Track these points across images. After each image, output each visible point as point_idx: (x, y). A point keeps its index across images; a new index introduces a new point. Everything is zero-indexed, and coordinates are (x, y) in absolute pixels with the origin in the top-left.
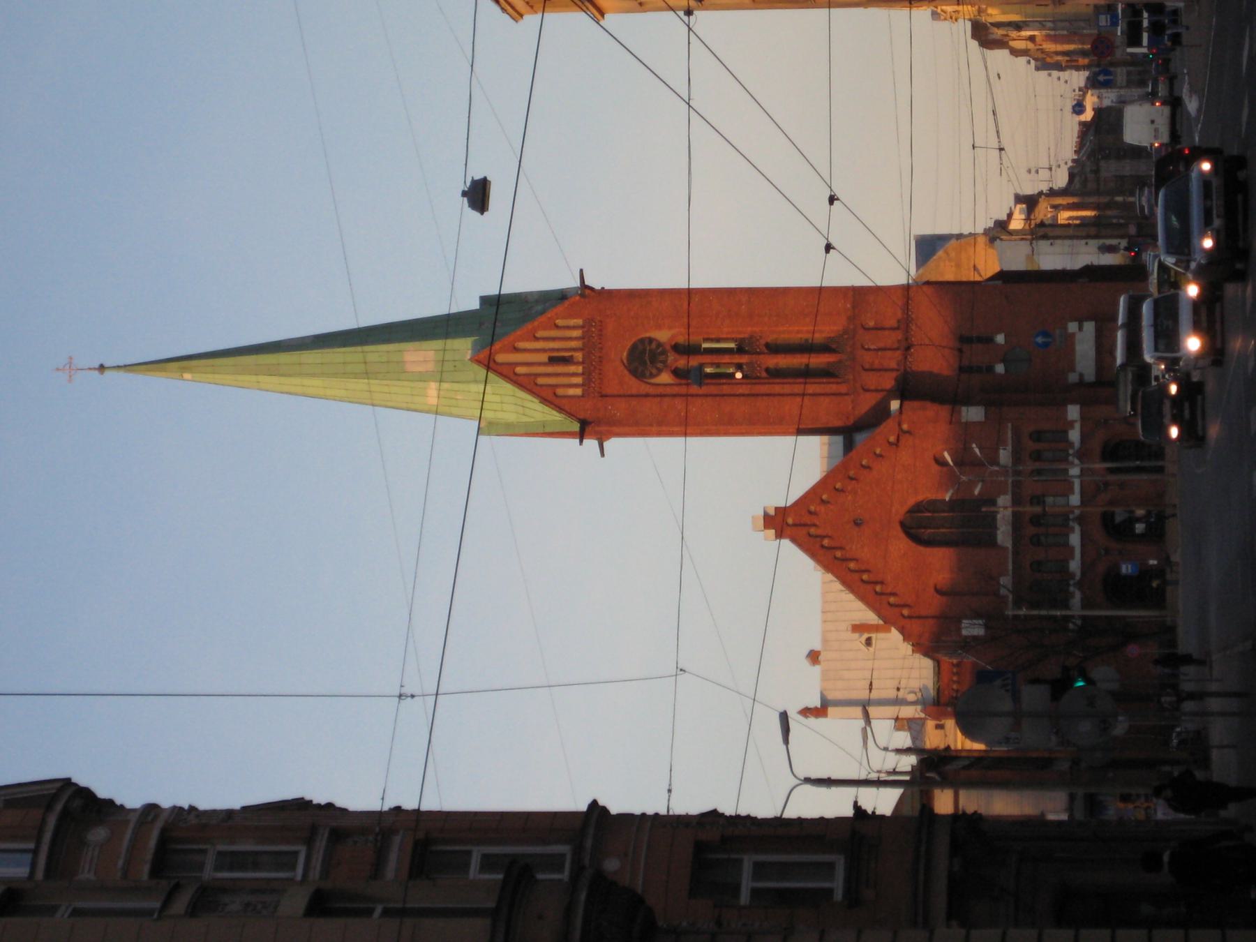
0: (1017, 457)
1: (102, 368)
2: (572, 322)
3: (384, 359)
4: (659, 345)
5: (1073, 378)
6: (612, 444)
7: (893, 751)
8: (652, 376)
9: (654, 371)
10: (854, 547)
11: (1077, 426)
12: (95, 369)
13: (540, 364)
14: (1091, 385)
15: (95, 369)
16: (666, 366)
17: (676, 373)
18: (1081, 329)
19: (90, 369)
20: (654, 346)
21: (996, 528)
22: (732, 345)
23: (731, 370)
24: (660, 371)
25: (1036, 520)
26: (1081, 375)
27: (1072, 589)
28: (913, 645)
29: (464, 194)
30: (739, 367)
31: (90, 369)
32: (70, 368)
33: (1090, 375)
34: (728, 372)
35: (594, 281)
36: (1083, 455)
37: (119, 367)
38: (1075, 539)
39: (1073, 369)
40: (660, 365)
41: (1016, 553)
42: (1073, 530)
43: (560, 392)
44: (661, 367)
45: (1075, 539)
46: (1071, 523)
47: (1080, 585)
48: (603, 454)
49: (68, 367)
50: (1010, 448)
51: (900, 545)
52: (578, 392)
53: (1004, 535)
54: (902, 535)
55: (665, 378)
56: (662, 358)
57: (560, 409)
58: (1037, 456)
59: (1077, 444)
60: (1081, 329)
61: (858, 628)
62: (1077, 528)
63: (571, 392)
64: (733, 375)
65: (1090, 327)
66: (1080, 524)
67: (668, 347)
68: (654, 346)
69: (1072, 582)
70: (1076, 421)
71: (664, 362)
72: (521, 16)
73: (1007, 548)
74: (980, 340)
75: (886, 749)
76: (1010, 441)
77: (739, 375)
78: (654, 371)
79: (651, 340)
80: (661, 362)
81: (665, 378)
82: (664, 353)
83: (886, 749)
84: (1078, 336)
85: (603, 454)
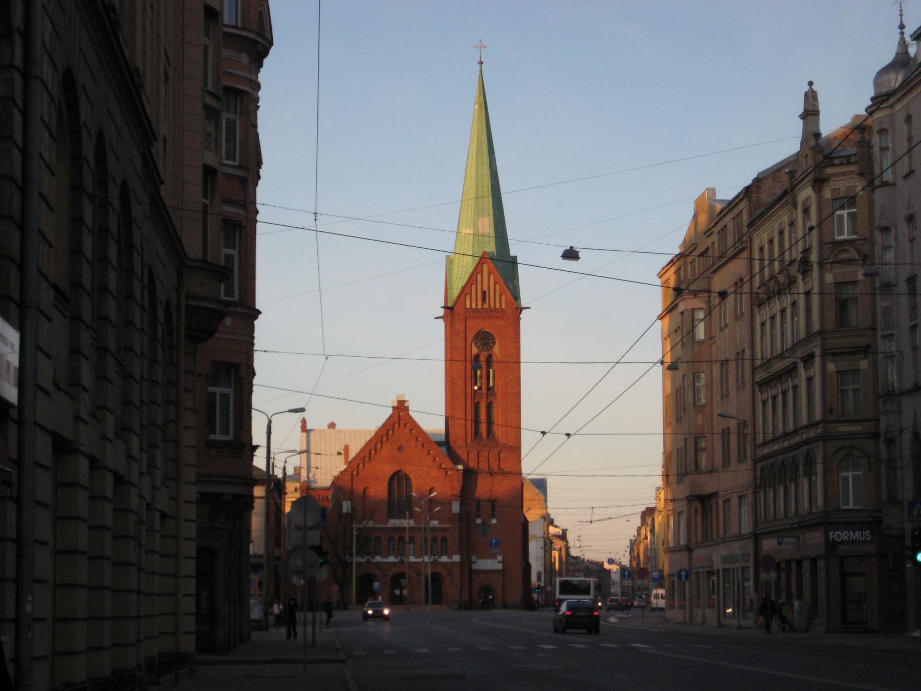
0: (434, 529)
1: (481, 63)
3: (485, 207)
4: (492, 347)
5: (474, 558)
6: (441, 323)
7: (285, 466)
8: (476, 344)
9: (478, 345)
11: (449, 560)
12: (481, 59)
13: (482, 286)
14: (470, 568)
15: (481, 59)
17: (477, 356)
18: (499, 562)
19: (481, 57)
20: (491, 345)
23: (478, 384)
24: (478, 348)
25: (401, 539)
26: (475, 562)
27: (366, 557)
28: (338, 476)
29: (572, 248)
30: (480, 388)
31: (481, 57)
32: (481, 47)
35: (524, 315)
37: (481, 71)
38: (392, 559)
39: (478, 558)
40: (481, 348)
41: (385, 529)
42: (396, 557)
43: (468, 297)
45: (392, 559)
46: (399, 557)
47: (368, 562)
48: (436, 318)
49: (482, 46)
50: (439, 526)
51: (389, 470)
52: (468, 306)
53: (394, 523)
54: (394, 471)
55: (475, 350)
56: (485, 349)
57: (459, 296)
58: (434, 540)
59: (440, 560)
60: (499, 562)
61: (346, 448)
62: (397, 560)
63: (468, 302)
64: (476, 384)
65: (500, 567)
66: (400, 562)
67: (490, 352)
68: (491, 345)
69: (370, 557)
70: (452, 559)
71: (483, 350)
72: (660, 278)
74: (493, 511)
75: (286, 462)
78: (478, 345)
79: (494, 343)
81: (475, 350)
82: (488, 350)
83: (286, 462)
84: (495, 561)
85: (436, 318)
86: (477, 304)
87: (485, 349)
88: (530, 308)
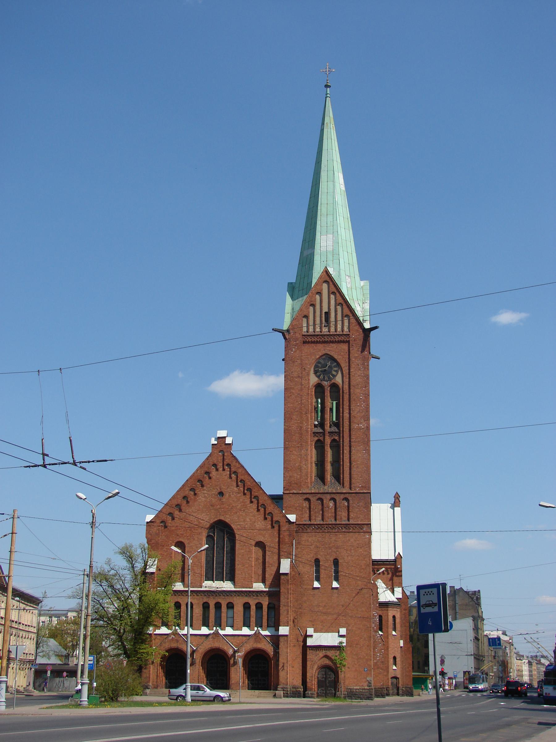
4: (334, 376)
5: (310, 631)
8: (316, 372)
9: (318, 374)
10: (205, 492)
11: (275, 633)
24: (318, 377)
33: (310, 642)
39: (315, 631)
40: (322, 377)
44: (321, 377)
52: (305, 329)
53: (209, 585)
55: (313, 380)
56: (326, 378)
67: (333, 381)
68: (334, 373)
71: (324, 380)
77: (316, 423)
80: (324, 377)
81: (313, 380)
82: (330, 379)
87: (326, 378)
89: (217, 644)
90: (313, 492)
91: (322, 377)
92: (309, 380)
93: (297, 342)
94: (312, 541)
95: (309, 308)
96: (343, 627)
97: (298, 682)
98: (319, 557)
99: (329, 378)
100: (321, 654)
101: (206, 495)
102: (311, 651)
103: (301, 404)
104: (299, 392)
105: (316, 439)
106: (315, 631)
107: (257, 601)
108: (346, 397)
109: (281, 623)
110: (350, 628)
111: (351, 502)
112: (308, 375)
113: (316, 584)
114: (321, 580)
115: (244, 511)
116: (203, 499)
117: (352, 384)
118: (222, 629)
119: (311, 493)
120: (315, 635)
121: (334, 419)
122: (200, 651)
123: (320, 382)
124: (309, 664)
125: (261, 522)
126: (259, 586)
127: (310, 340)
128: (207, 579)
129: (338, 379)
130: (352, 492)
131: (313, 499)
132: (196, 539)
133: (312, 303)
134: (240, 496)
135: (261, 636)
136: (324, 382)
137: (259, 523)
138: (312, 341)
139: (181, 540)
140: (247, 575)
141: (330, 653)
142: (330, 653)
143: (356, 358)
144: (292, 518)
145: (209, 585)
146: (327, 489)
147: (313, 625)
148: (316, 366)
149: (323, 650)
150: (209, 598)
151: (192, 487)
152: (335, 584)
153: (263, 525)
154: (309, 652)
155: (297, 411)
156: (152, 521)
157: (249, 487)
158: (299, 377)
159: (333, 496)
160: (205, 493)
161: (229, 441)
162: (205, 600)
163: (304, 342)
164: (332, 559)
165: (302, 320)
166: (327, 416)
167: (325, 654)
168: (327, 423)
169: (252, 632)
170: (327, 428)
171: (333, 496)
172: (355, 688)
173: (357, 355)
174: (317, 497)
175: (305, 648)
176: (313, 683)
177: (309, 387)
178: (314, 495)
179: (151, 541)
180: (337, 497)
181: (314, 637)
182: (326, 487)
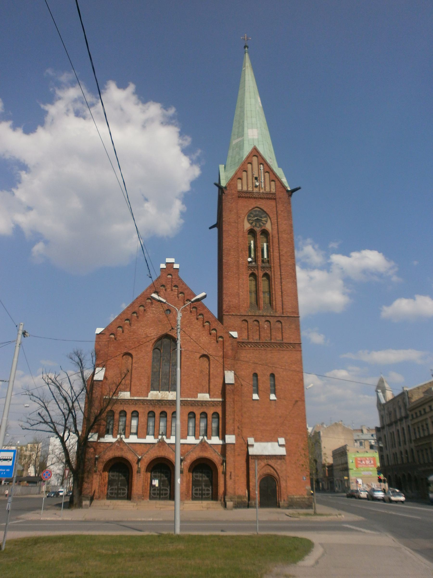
2: (273, 187)
5: (251, 441)
8: (248, 220)
16: (254, 227)
18: (280, 446)
21: (159, 390)
22: (265, 256)
23: (252, 256)
24: (251, 224)
26: (252, 446)
33: (252, 451)
34: (252, 255)
36: (203, 444)
39: (256, 441)
40: (254, 224)
44: (253, 224)
45: (150, 439)
47: (120, 441)
50: (210, 400)
52: (239, 188)
53: (154, 395)
55: (247, 226)
56: (258, 225)
59: (209, 442)
64: (250, 256)
65: (282, 451)
67: (263, 228)
73: (147, 396)
76: (213, 400)
77: (250, 259)
80: (256, 224)
82: (260, 226)
84: (276, 444)
86: (247, 188)
87: (258, 225)
88: (299, 188)
89: (162, 453)
90: (250, 314)
91: (254, 224)
92: (244, 225)
93: (234, 196)
94: (250, 357)
95: (242, 173)
96: (281, 437)
97: (242, 491)
98: (257, 372)
99: (260, 226)
100: (263, 463)
101: (154, 312)
102: (253, 460)
103: (238, 243)
104: (236, 234)
105: (250, 272)
106: (256, 441)
107: (202, 410)
108: (276, 240)
109: (227, 432)
110: (288, 438)
111: (283, 324)
112: (243, 221)
113: (255, 397)
114: (260, 392)
115: (190, 327)
116: (152, 315)
117: (279, 230)
118: (167, 438)
119: (249, 315)
120: (256, 444)
121: (265, 256)
122: (145, 460)
123: (252, 228)
124: (251, 472)
125: (205, 337)
126: (204, 397)
127: (244, 196)
128: (152, 389)
129: (268, 227)
130: (284, 316)
131: (250, 321)
132: (143, 351)
133: (245, 169)
134: (186, 313)
135: (207, 445)
136: (256, 228)
137: (204, 338)
138: (245, 196)
139: (130, 352)
140: (192, 385)
141: (272, 462)
142: (272, 462)
143: (282, 211)
144: (235, 334)
145: (154, 395)
146: (261, 312)
147: (253, 435)
148: (249, 216)
149: (264, 459)
150: (155, 407)
151: (141, 304)
152: (273, 397)
153: (207, 340)
154: (251, 461)
155: (234, 249)
156: (102, 333)
157: (195, 306)
158: (235, 222)
159: (268, 318)
160: (154, 310)
161: (176, 266)
162: (151, 409)
163: (239, 197)
164: (269, 374)
165: (237, 181)
166: (259, 254)
167: (266, 463)
168: (260, 259)
169: (198, 442)
170: (260, 263)
171: (268, 318)
172: (295, 497)
173: (282, 209)
174: (254, 319)
175: (248, 456)
176: (256, 493)
177: (244, 231)
178: (251, 317)
179: (100, 352)
180: (272, 320)
181: (255, 446)
182: (261, 312)
